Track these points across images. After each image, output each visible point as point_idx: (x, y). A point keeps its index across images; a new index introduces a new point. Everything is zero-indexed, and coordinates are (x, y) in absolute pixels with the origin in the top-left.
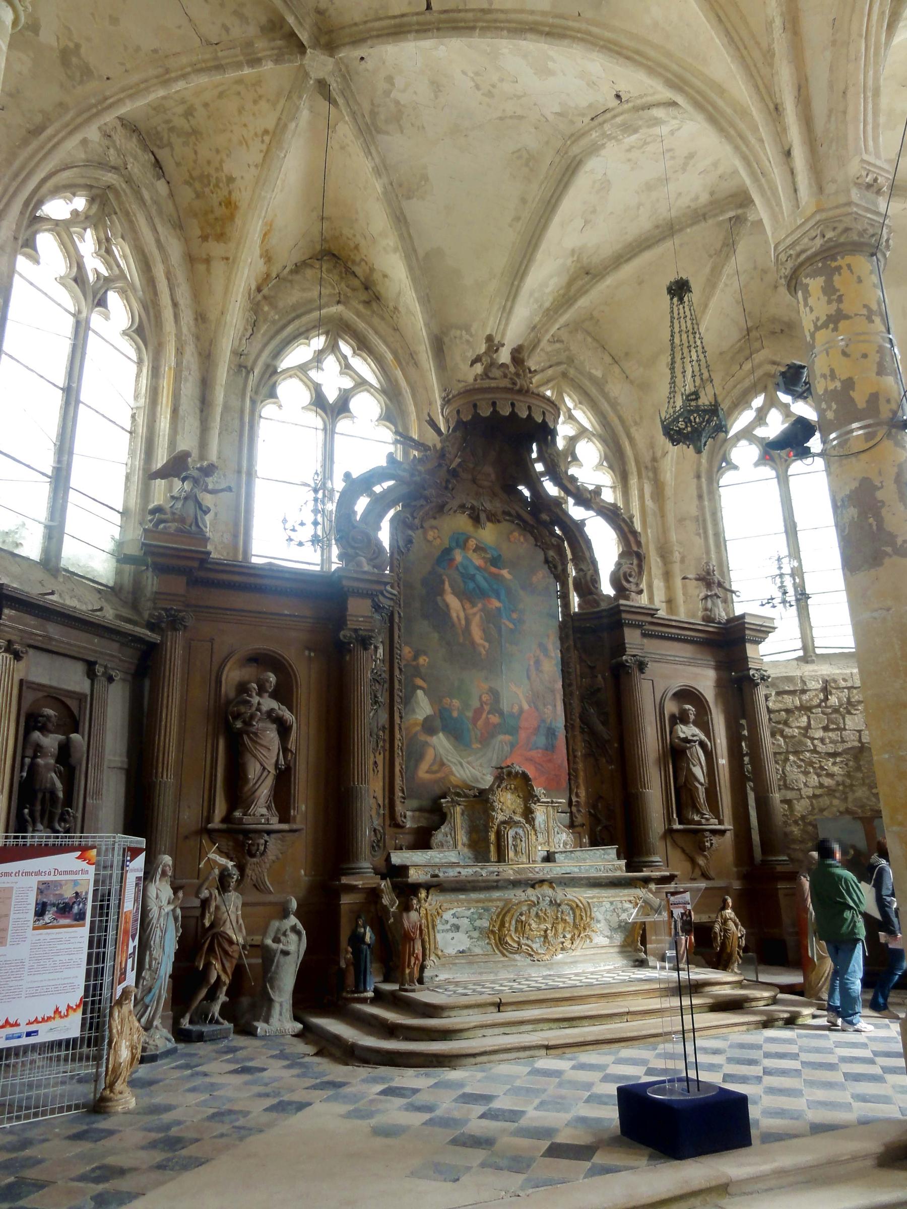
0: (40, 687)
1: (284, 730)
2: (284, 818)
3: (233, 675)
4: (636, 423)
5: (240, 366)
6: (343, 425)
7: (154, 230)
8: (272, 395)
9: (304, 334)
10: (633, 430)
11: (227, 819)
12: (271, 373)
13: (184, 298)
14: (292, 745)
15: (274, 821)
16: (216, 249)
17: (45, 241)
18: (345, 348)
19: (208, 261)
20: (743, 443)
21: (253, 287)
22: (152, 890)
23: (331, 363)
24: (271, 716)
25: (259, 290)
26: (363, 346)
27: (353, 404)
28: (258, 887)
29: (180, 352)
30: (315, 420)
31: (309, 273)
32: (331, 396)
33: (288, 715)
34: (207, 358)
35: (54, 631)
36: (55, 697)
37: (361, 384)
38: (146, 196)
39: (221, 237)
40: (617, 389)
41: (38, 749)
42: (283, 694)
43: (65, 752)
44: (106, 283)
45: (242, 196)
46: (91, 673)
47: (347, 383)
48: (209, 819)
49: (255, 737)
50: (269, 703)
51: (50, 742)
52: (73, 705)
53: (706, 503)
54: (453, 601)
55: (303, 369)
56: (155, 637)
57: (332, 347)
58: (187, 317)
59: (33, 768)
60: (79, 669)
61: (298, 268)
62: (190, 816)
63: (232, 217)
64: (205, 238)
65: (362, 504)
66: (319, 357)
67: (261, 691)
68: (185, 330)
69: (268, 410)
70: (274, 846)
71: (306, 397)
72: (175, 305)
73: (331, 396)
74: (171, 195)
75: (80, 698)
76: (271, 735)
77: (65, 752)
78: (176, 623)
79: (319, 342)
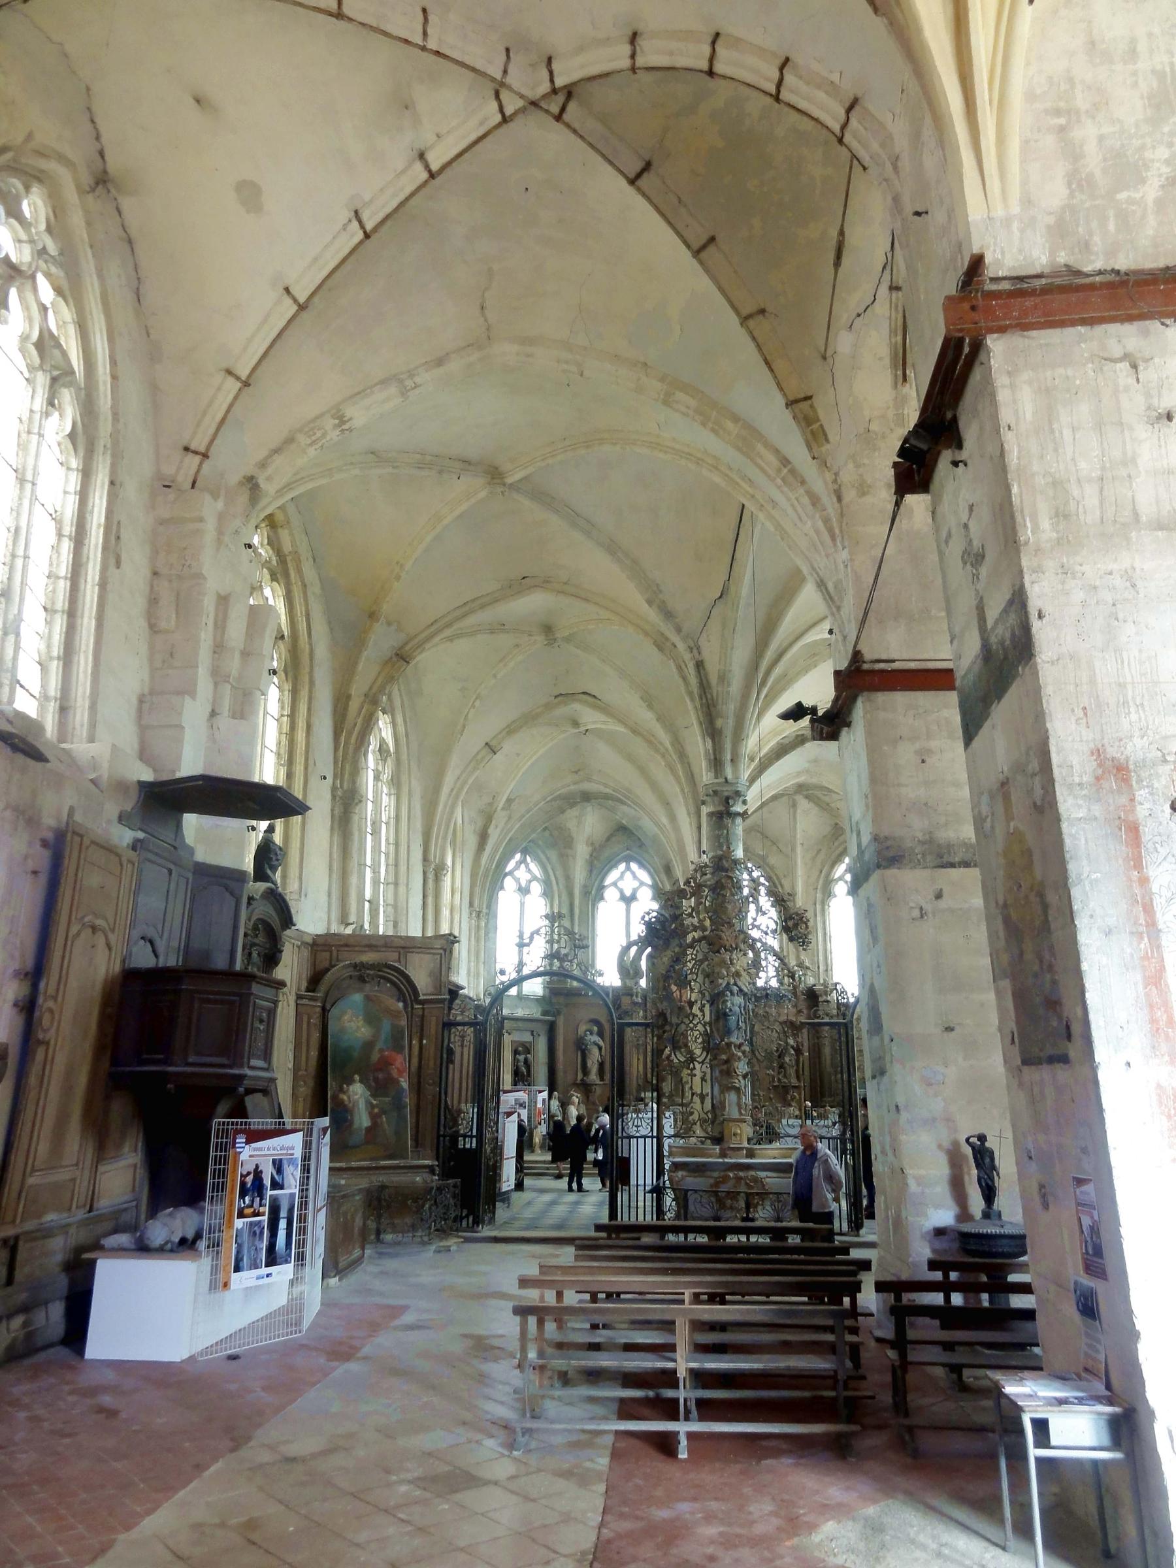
0: (516, 1042)
1: (600, 1048)
2: (602, 1079)
3: (582, 1029)
4: (785, 876)
5: (586, 893)
6: (634, 905)
7: (544, 852)
8: (602, 898)
9: (615, 866)
10: (783, 881)
11: (582, 1080)
12: (602, 888)
13: (559, 873)
14: (603, 1053)
15: (598, 1082)
16: (569, 852)
17: (509, 882)
18: (634, 866)
19: (567, 856)
20: (841, 883)
21: (588, 857)
22: (552, 1102)
23: (628, 874)
24: (595, 1044)
25: (591, 855)
26: (642, 865)
27: (638, 895)
28: (594, 1104)
29: (560, 897)
30: (623, 905)
31: (614, 839)
32: (628, 893)
33: (601, 1043)
34: (571, 895)
35: (520, 1024)
36: (523, 1044)
37: (642, 884)
38: (540, 843)
39: (571, 848)
40: (773, 860)
41: (518, 1061)
42: (601, 1034)
43: (526, 1061)
44: (530, 881)
45: (574, 835)
46: (533, 1035)
47: (636, 884)
48: (576, 1079)
49: (589, 1051)
50: (595, 1038)
51: (521, 1058)
52: (528, 1045)
53: (818, 918)
54: (674, 988)
55: (615, 884)
56: (554, 1019)
57: (628, 868)
58: (562, 881)
59: (517, 1067)
60: (529, 1034)
61: (608, 839)
62: (570, 1079)
63: (572, 842)
64: (565, 848)
65: (633, 950)
66: (623, 874)
67: (591, 1034)
68: (561, 887)
69: (601, 906)
70: (598, 1091)
71: (618, 895)
72: (556, 879)
73: (628, 893)
74: (551, 835)
75: (530, 1043)
76: (596, 1051)
77: (526, 1061)
78: (559, 1013)
79: (622, 866)
